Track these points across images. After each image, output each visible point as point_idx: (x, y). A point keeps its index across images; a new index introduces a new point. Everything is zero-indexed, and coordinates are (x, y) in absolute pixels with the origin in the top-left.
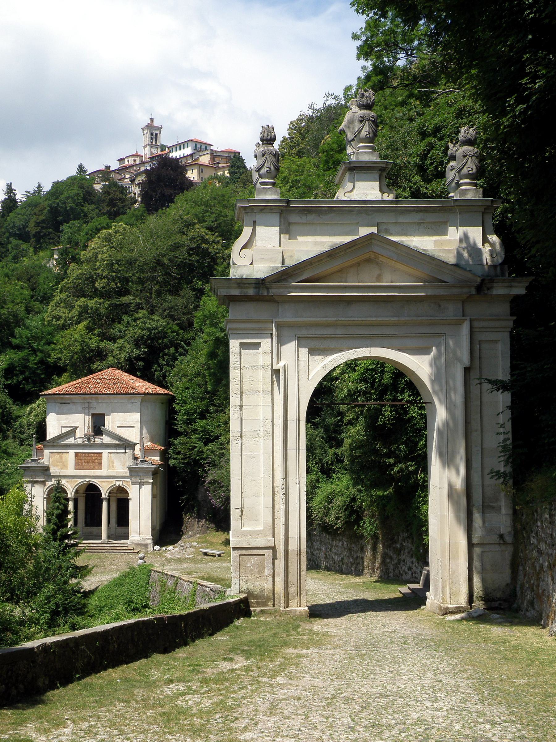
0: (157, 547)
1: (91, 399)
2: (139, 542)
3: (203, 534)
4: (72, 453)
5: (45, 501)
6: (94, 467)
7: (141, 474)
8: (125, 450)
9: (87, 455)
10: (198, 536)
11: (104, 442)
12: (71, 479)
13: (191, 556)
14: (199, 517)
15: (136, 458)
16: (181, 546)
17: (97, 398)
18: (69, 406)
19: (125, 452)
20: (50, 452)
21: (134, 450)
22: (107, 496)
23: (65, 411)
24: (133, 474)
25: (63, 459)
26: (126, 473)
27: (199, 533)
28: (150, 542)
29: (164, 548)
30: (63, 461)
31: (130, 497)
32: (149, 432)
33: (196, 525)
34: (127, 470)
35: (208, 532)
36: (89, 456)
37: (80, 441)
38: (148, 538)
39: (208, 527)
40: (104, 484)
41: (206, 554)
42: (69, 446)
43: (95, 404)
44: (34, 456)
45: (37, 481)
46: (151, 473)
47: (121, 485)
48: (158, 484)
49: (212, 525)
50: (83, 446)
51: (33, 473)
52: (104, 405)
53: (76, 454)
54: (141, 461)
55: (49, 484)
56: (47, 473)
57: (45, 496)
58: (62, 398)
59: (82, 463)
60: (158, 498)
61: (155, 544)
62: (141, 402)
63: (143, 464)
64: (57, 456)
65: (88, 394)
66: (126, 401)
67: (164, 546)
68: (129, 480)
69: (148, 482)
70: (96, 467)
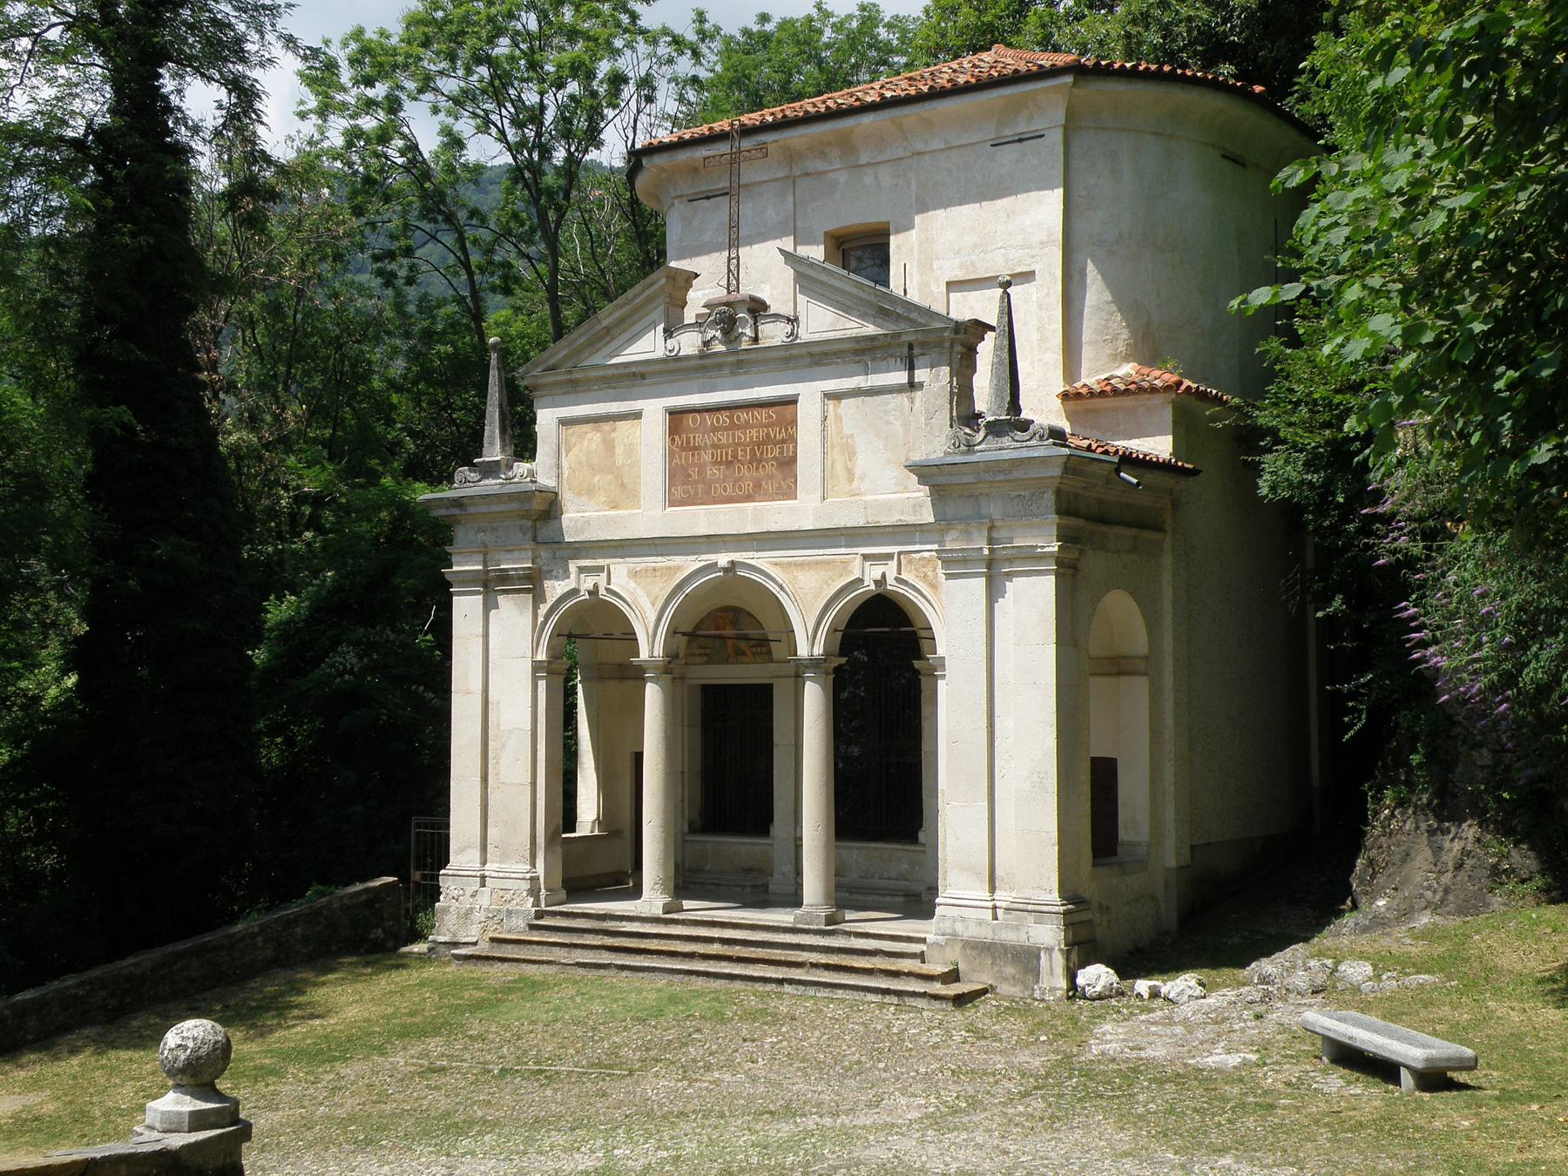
0: (1097, 976)
1: (820, 150)
2: (986, 934)
3: (1462, 911)
4: (654, 409)
5: (542, 684)
9: (724, 417)
10: (1424, 920)
11: (805, 335)
13: (1234, 1060)
14: (1448, 810)
15: (969, 418)
16: (1264, 980)
17: (846, 144)
19: (912, 385)
21: (965, 365)
22: (818, 650)
23: (707, 237)
24: (950, 511)
25: (619, 450)
26: (917, 506)
27: (1435, 908)
28: (1049, 935)
29: (1142, 986)
30: (620, 460)
32: (1126, 301)
33: (1423, 856)
34: (922, 493)
35: (1497, 900)
36: (733, 426)
37: (689, 344)
39: (1495, 871)
41: (1349, 1057)
42: (640, 378)
43: (843, 177)
44: (492, 443)
45: (504, 577)
46: (1049, 498)
47: (892, 584)
48: (1167, 594)
49: (1522, 859)
50: (701, 368)
52: (886, 176)
53: (675, 415)
54: (996, 429)
55: (555, 589)
56: (545, 532)
57: (542, 656)
58: (693, 171)
59: (701, 472)
60: (1168, 680)
61: (1082, 949)
62: (1070, 130)
63: (1006, 441)
64: (592, 438)
66: (991, 133)
67: (1147, 973)
69: (1031, 556)
70: (769, 486)
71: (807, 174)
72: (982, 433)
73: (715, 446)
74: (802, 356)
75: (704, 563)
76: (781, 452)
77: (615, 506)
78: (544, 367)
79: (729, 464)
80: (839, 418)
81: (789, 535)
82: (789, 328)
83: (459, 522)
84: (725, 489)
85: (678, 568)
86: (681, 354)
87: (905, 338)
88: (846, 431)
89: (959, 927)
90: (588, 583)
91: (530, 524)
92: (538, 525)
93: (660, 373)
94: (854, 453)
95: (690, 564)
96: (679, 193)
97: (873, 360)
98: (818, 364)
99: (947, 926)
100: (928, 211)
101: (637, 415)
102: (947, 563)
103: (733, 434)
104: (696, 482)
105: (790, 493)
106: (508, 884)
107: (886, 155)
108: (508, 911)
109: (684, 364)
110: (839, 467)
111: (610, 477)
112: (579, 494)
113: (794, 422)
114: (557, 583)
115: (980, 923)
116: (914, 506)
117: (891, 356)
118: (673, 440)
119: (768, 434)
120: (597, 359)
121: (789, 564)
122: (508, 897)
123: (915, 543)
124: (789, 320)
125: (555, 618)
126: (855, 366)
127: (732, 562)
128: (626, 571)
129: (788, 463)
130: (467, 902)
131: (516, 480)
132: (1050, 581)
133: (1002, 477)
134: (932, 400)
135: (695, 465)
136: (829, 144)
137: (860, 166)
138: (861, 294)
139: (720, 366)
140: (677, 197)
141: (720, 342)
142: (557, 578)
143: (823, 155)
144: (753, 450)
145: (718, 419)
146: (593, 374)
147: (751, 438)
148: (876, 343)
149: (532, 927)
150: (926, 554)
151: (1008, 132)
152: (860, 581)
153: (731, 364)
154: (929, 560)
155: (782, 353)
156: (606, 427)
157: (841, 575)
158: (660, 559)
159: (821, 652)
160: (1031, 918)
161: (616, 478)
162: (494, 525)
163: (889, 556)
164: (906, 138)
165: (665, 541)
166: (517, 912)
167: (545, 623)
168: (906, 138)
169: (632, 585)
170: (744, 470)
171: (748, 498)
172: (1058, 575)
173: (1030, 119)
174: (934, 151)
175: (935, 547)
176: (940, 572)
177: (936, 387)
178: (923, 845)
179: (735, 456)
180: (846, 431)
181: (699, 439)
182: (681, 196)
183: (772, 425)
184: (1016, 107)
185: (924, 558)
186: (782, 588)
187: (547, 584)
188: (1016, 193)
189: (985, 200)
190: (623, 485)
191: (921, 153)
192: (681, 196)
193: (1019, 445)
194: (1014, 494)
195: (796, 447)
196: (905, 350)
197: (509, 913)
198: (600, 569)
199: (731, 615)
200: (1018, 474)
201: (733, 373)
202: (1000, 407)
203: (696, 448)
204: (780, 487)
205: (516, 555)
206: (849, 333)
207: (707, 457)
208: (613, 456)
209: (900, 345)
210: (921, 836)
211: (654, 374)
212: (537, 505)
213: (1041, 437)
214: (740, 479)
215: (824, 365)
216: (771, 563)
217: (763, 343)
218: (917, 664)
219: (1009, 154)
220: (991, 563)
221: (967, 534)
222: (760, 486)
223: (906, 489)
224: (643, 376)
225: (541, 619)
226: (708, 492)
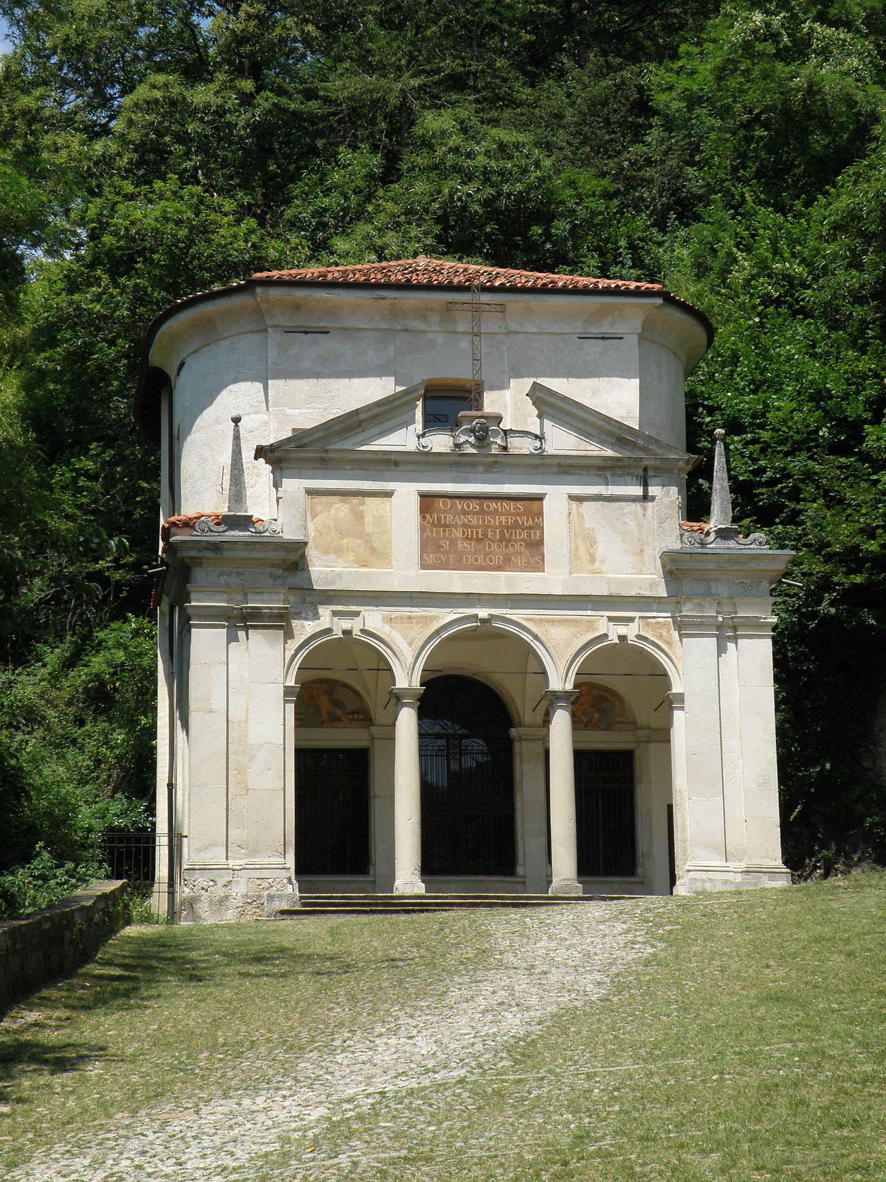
1: (422, 314)
5: (291, 707)
7: (722, 590)
8: (646, 485)
9: (474, 505)
12: (406, 611)
18: (328, 345)
19: (645, 498)
20: (310, 492)
22: (569, 686)
23: (305, 365)
24: (686, 587)
25: (368, 520)
26: (653, 585)
30: (369, 528)
31: (675, 689)
36: (482, 512)
38: (772, 873)
43: (440, 339)
46: (766, 586)
47: (632, 639)
51: (233, 580)
55: (304, 628)
56: (297, 579)
57: (291, 682)
58: (296, 307)
59: (453, 542)
63: (732, 544)
64: (340, 509)
65: (420, 287)
66: (579, 328)
68: (664, 617)
69: (755, 625)
71: (407, 330)
72: (712, 536)
73: (465, 526)
74: (550, 465)
75: (458, 616)
76: (529, 536)
78: (297, 444)
79: (479, 541)
80: (580, 515)
81: (543, 598)
82: (538, 444)
83: (200, 565)
84: (476, 560)
85: (434, 618)
86: (433, 451)
88: (587, 525)
89: (708, 887)
90: (346, 624)
91: (281, 572)
92: (285, 574)
93: (414, 463)
94: (595, 543)
95: (447, 615)
96: (276, 323)
97: (613, 475)
98: (565, 473)
99: (698, 886)
100: (523, 377)
101: (388, 494)
102: (680, 626)
103: (483, 519)
104: (447, 552)
105: (539, 567)
106: (266, 874)
108: (269, 896)
109: (443, 458)
110: (582, 551)
111: (359, 541)
112: (326, 552)
113: (540, 514)
114: (306, 623)
115: (726, 882)
116: (651, 585)
117: (629, 474)
118: (424, 518)
119: (516, 521)
120: (347, 445)
121: (541, 620)
122: (265, 884)
123: (652, 611)
124: (536, 437)
125: (304, 653)
126: (597, 478)
127: (491, 615)
128: (380, 618)
129: (537, 545)
130: (219, 891)
131: (267, 534)
132: (769, 643)
133: (737, 567)
134: (664, 510)
135: (447, 539)
136: (432, 310)
137: (457, 332)
138: (607, 426)
139: (474, 465)
140: (273, 326)
141: (473, 446)
142: (306, 619)
143: (424, 317)
144: (502, 532)
146: (351, 456)
147: (501, 522)
148: (620, 463)
149: (305, 905)
150: (661, 620)
151: (593, 330)
152: (605, 636)
153: (485, 464)
154: (664, 624)
155: (537, 461)
156: (355, 500)
157: (588, 631)
158: (416, 609)
159: (572, 687)
160: (766, 877)
161: (366, 542)
162: (240, 570)
164: (504, 319)
165: (424, 595)
166: (280, 896)
168: (504, 319)
170: (494, 547)
171: (499, 568)
172: (773, 637)
173: (613, 324)
174: (527, 333)
175: (669, 615)
176: (676, 634)
177: (667, 501)
178: (524, 877)
179: (485, 535)
180: (587, 525)
181: (449, 519)
182: (277, 326)
183: (520, 515)
184: (602, 314)
185: (659, 623)
186: (536, 637)
187: (295, 623)
188: (599, 376)
189: (573, 377)
190: (373, 549)
191: (516, 332)
192: (277, 326)
193: (742, 547)
194: (737, 581)
195: (542, 533)
196: (641, 472)
197: (271, 898)
198: (357, 614)
199: (325, 687)
200: (752, 565)
201: (486, 471)
202: (725, 519)
203: (446, 526)
204: (528, 562)
205: (266, 597)
206: (590, 453)
207: (458, 533)
208: (362, 524)
210: (520, 870)
211: (407, 463)
212: (294, 557)
213: (761, 543)
214: (490, 553)
215: (570, 474)
216: (524, 619)
217: (511, 451)
218: (513, 732)
219: (593, 348)
220: (719, 627)
221: (701, 606)
222: (510, 560)
223: (641, 572)
224: (396, 464)
225: (289, 654)
226: (460, 561)
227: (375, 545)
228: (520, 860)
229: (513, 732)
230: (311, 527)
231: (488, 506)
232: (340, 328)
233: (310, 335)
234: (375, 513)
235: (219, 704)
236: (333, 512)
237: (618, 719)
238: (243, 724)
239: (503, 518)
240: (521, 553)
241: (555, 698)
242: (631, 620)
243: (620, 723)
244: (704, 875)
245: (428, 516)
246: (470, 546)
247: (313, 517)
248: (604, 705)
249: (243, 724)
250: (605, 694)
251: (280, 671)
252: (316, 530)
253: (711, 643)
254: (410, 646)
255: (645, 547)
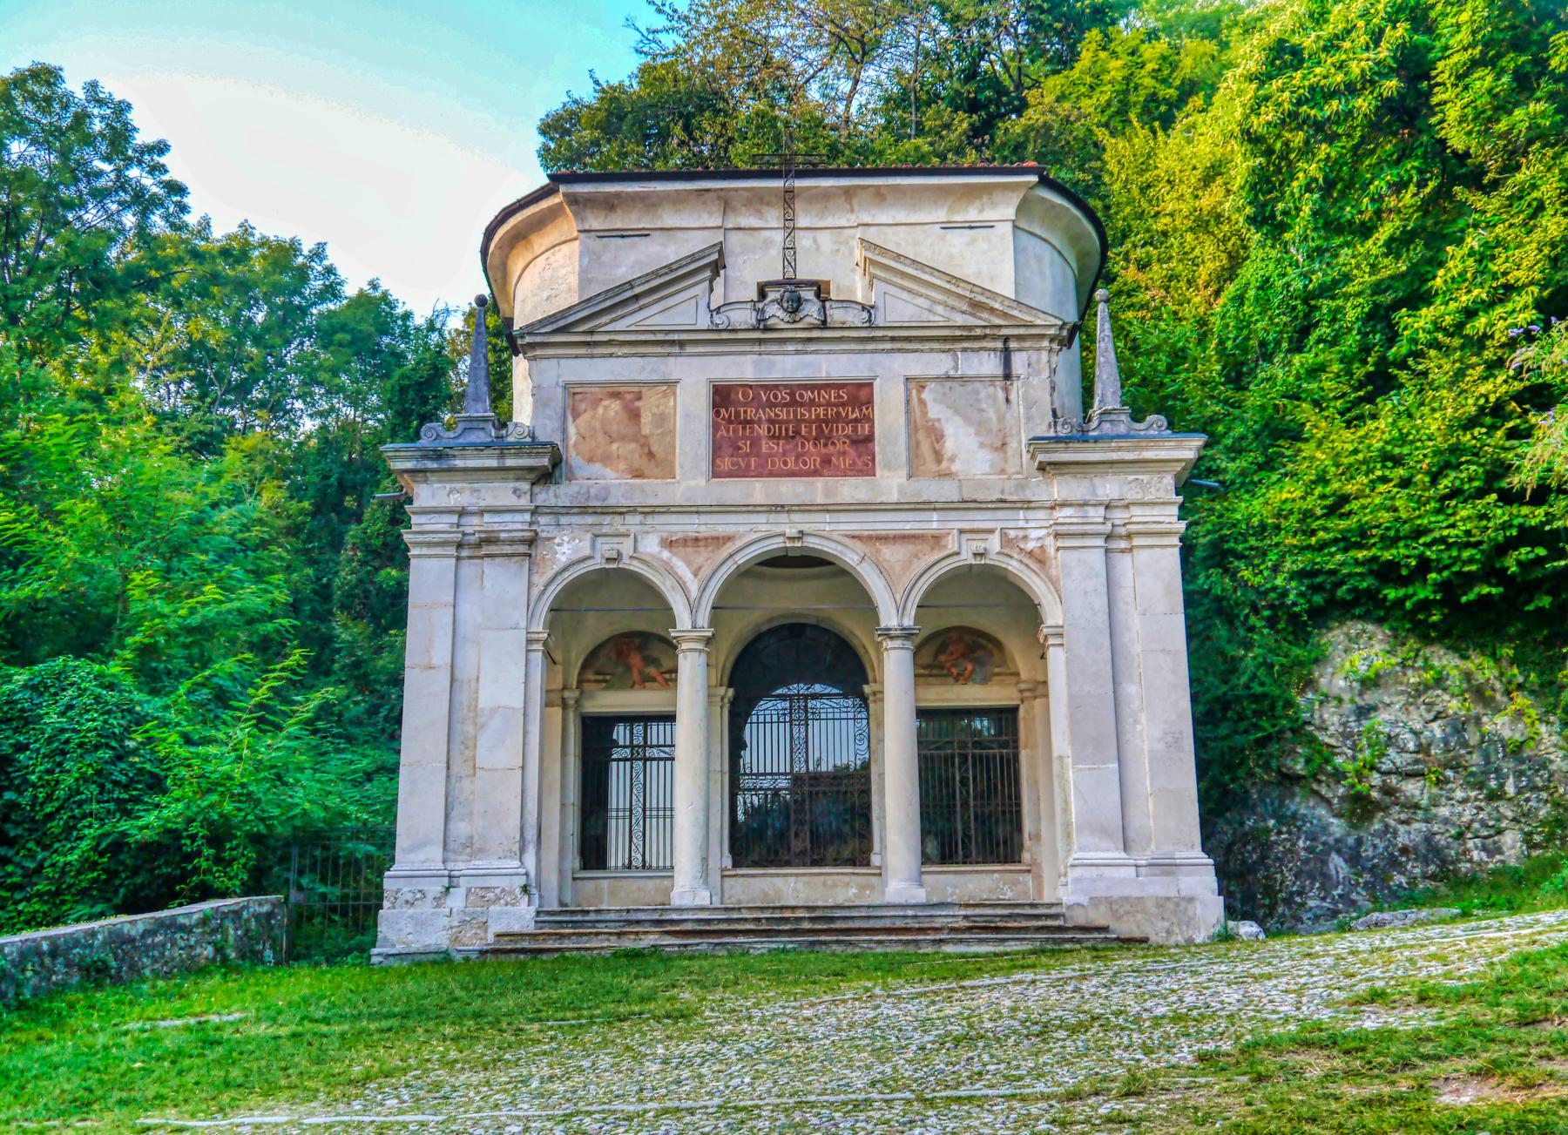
6: (827, 461)
22: (908, 622)
25: (646, 418)
30: (646, 429)
36: (794, 403)
40: (892, 554)
57: (539, 627)
59: (755, 443)
73: (771, 421)
76: (855, 430)
77: (639, 474)
80: (922, 402)
84: (785, 463)
85: (729, 539)
87: (1005, 332)
94: (942, 436)
96: (587, 227)
103: (795, 413)
104: (747, 455)
105: (868, 469)
106: (492, 882)
107: (829, 221)
110: (925, 448)
111: (633, 445)
113: (870, 402)
118: (717, 414)
121: (870, 538)
128: (657, 540)
132: (1176, 551)
144: (819, 428)
145: (776, 397)
147: (818, 415)
151: (958, 218)
161: (643, 446)
163: (991, 531)
167: (539, 599)
169: (666, 554)
170: (809, 446)
171: (815, 473)
173: (981, 211)
179: (797, 432)
180: (931, 415)
183: (843, 405)
190: (651, 455)
195: (872, 427)
196: (1000, 345)
199: (637, 641)
204: (854, 463)
207: (762, 431)
208: (638, 424)
209: (995, 338)
210: (875, 859)
214: (804, 454)
218: (867, 689)
222: (829, 461)
225: (536, 591)
227: (654, 449)
228: (876, 847)
229: (867, 689)
230: (572, 430)
231: (801, 396)
232: (661, 229)
233: (627, 240)
234: (655, 410)
235: (441, 656)
236: (600, 410)
237: (997, 670)
238: (473, 683)
239: (821, 411)
240: (844, 453)
241: (888, 634)
242: (991, 531)
243: (998, 674)
244: (1095, 872)
245: (723, 411)
246: (779, 448)
247: (576, 416)
248: (979, 653)
249: (473, 683)
250: (984, 642)
251: (520, 617)
252: (578, 434)
253: (1096, 558)
254: (696, 575)
255: (1008, 440)
